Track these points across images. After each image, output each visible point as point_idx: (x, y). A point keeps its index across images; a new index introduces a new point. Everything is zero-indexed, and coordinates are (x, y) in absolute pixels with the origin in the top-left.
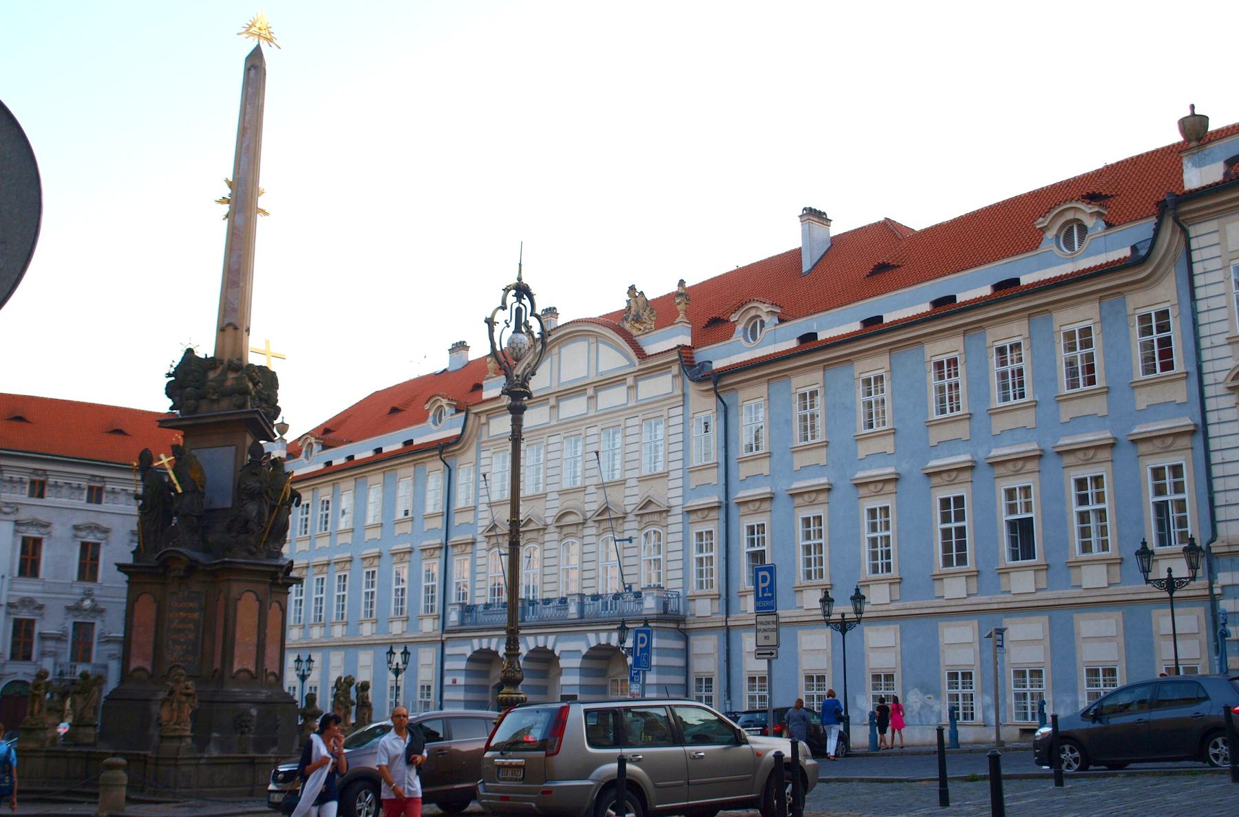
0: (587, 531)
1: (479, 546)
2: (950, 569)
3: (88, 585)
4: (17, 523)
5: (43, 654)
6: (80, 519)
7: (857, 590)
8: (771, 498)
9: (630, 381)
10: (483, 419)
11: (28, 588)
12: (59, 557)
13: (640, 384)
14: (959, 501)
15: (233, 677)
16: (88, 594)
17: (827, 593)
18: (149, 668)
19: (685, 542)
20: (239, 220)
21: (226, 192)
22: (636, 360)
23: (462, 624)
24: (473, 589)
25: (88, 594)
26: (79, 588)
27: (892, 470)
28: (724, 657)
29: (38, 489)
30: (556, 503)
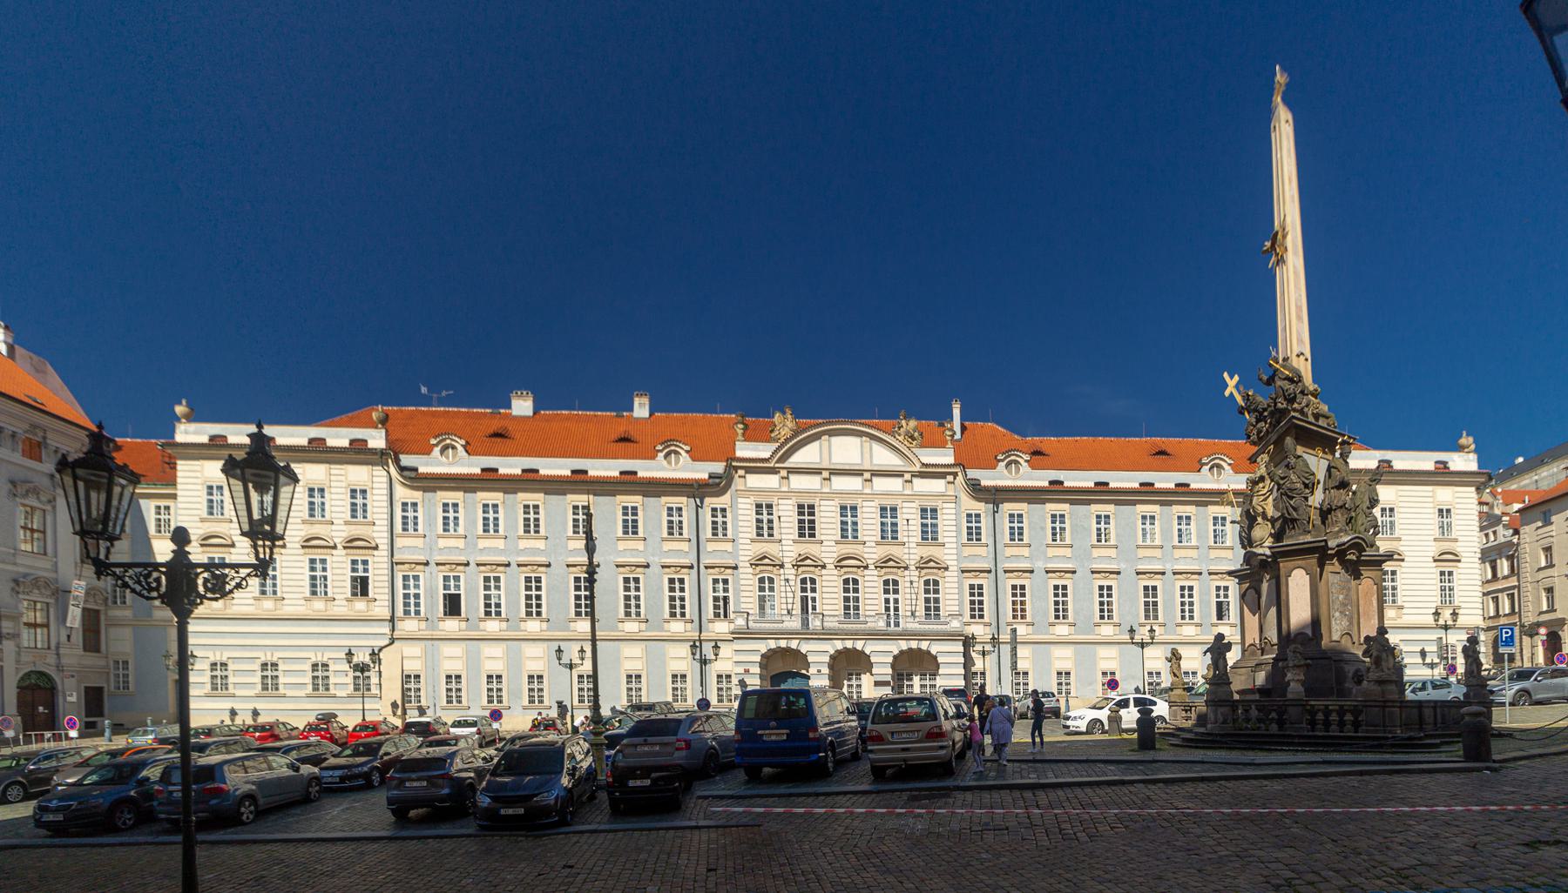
10: (741, 472)
14: (1154, 588)
19: (960, 588)
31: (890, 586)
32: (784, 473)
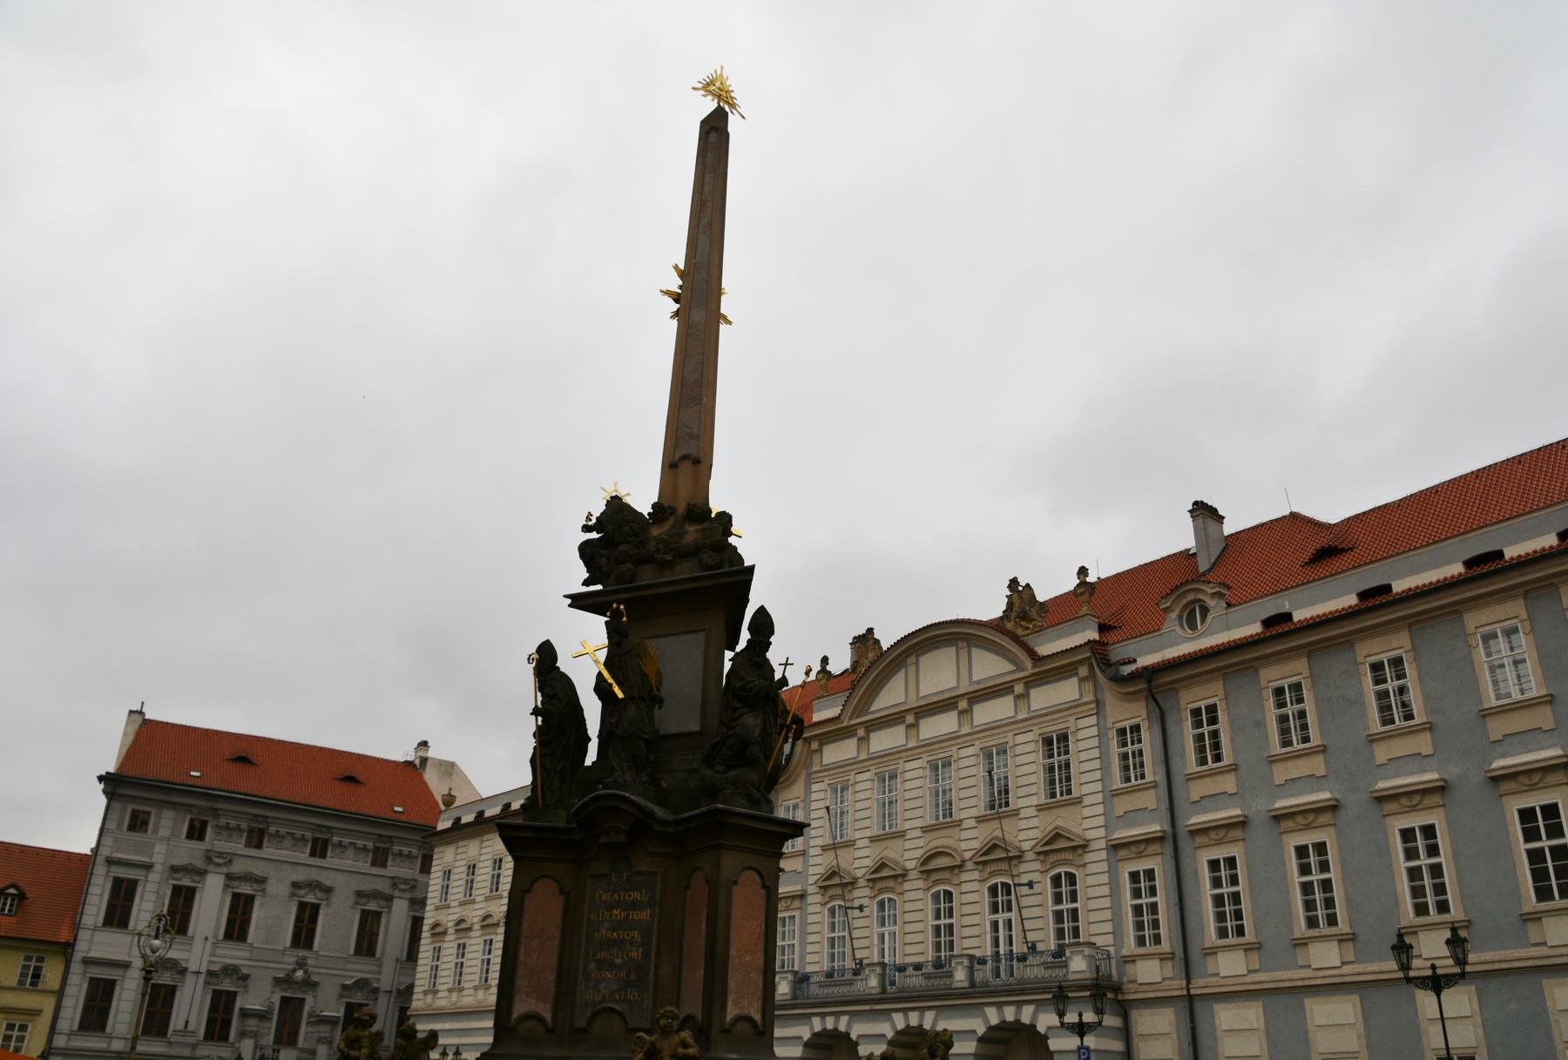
0: (965, 876)
1: (810, 899)
2: (1550, 905)
3: (303, 953)
4: (229, 877)
5: (243, 1034)
6: (300, 875)
7: (1400, 936)
8: (1242, 823)
9: (1019, 688)
10: (815, 745)
11: (233, 955)
12: (272, 919)
13: (1034, 692)
15: (727, 1031)
16: (301, 964)
17: (1454, 930)
18: (548, 1017)
19: (1114, 884)
20: (698, 316)
21: (675, 283)
22: (1028, 663)
23: (795, 997)
24: (803, 953)
25: (301, 964)
26: (290, 959)
27: (1435, 776)
28: (1187, 1039)
29: (256, 839)
30: (920, 842)
31: (1001, 898)
32: (861, 732)
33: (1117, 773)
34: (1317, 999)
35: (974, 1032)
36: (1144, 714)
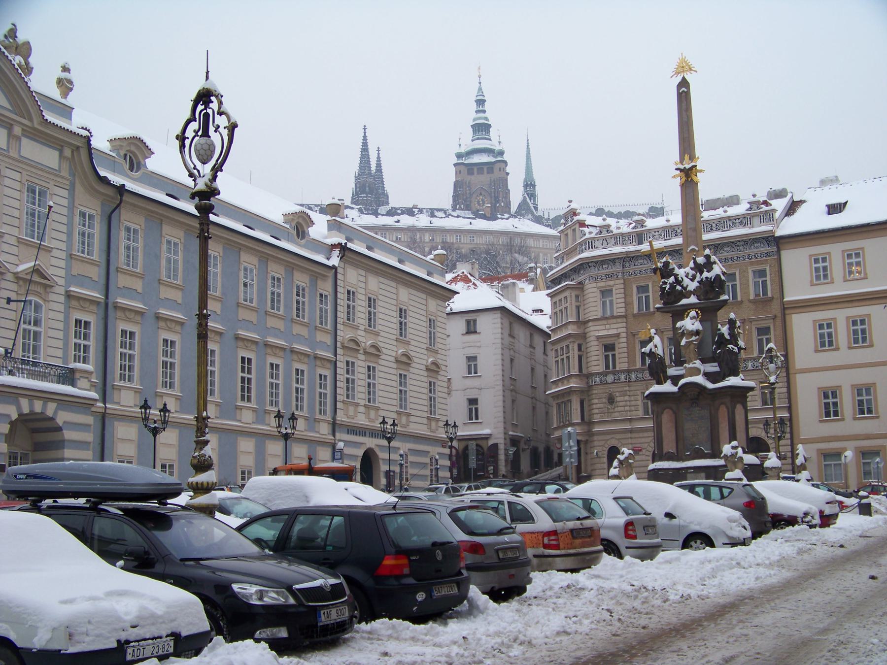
8: (141, 313)
33: (76, 246)
34: (121, 423)
35: (8, 416)
36: (99, 213)
